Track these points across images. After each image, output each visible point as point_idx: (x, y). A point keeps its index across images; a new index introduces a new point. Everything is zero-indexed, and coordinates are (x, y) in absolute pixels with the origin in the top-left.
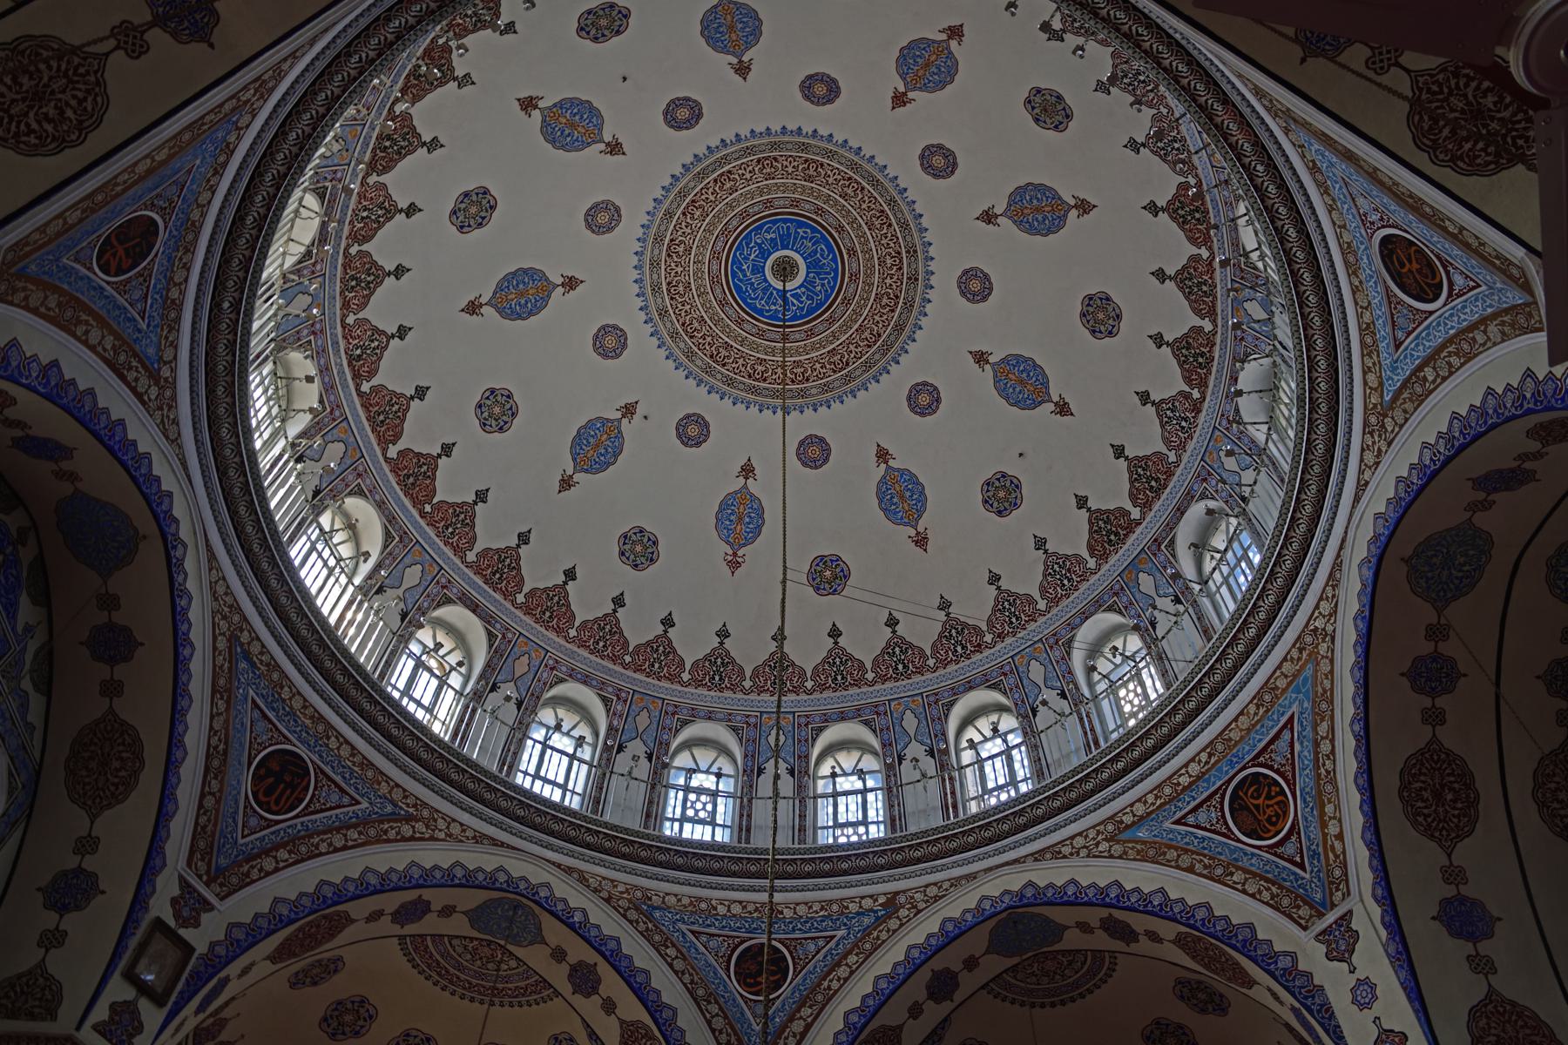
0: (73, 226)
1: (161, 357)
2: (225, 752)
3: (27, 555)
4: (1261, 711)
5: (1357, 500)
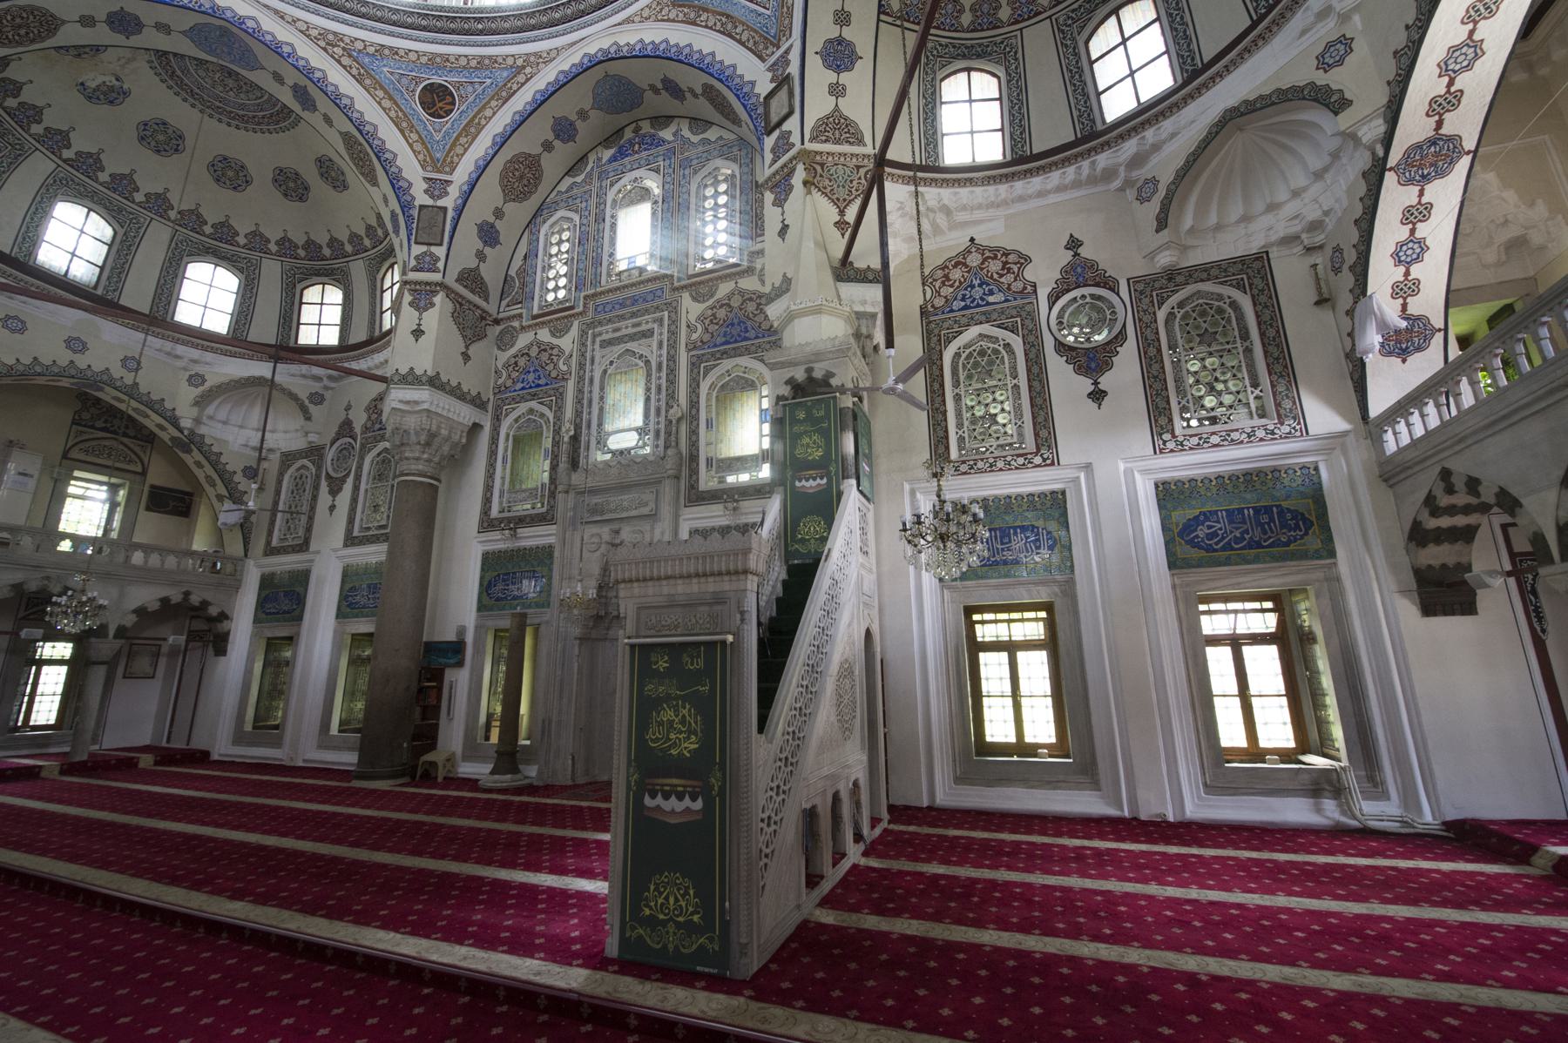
0: (420, 137)
1: (512, 67)
2: (728, 16)
3: (646, 127)
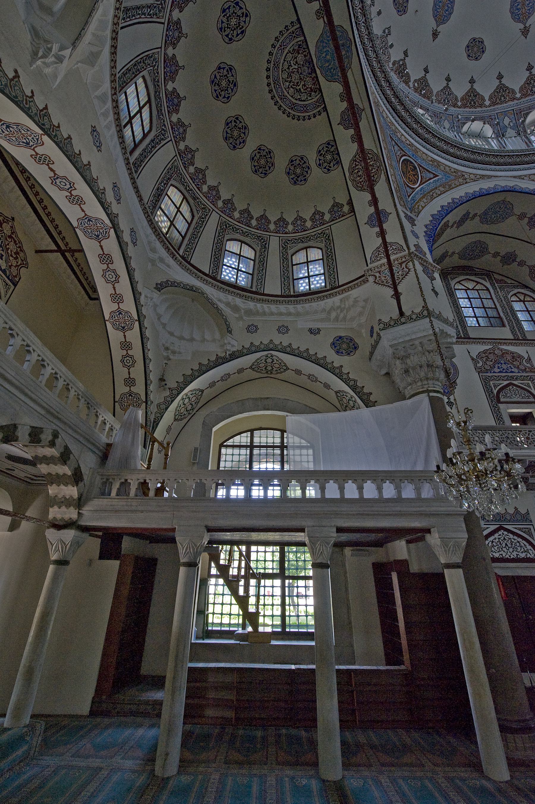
4: (431, 163)
5: (515, 177)
